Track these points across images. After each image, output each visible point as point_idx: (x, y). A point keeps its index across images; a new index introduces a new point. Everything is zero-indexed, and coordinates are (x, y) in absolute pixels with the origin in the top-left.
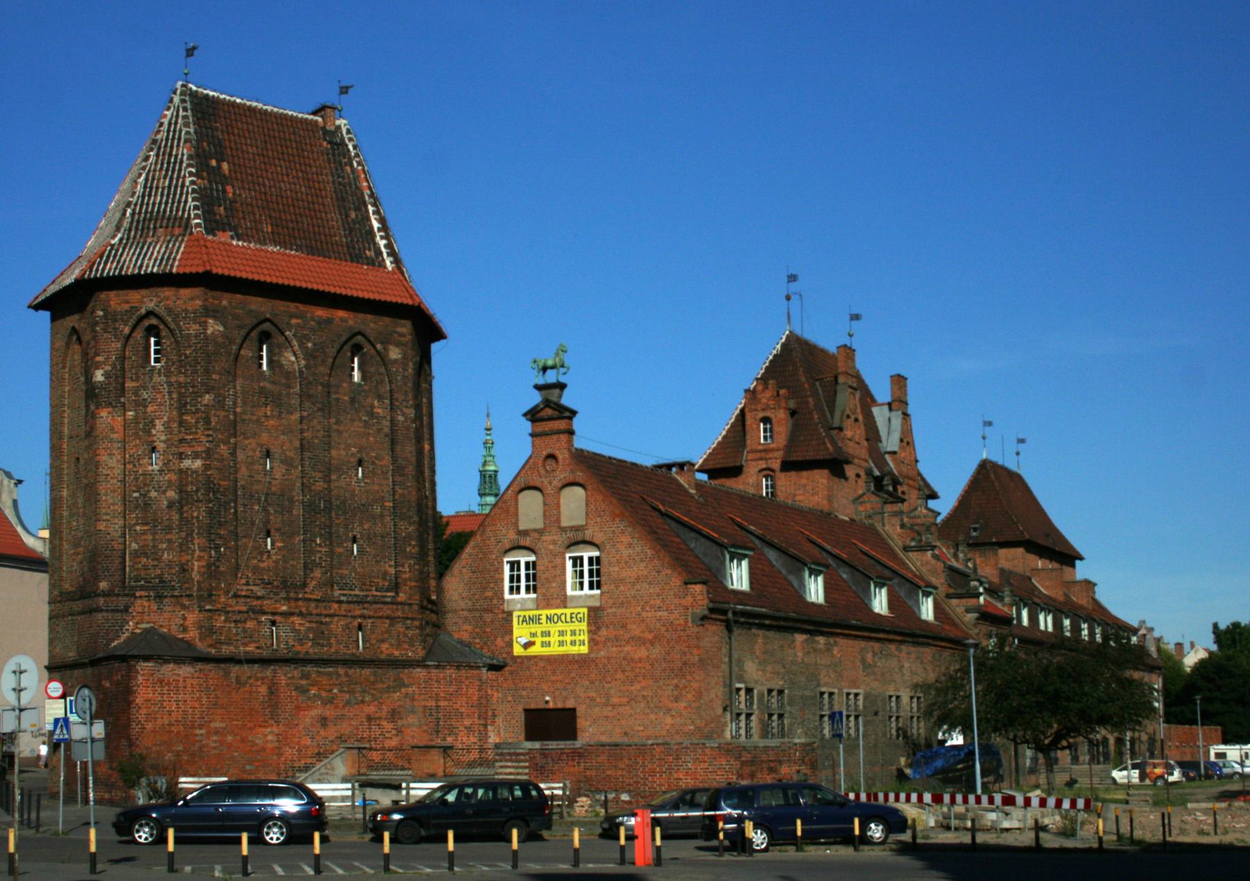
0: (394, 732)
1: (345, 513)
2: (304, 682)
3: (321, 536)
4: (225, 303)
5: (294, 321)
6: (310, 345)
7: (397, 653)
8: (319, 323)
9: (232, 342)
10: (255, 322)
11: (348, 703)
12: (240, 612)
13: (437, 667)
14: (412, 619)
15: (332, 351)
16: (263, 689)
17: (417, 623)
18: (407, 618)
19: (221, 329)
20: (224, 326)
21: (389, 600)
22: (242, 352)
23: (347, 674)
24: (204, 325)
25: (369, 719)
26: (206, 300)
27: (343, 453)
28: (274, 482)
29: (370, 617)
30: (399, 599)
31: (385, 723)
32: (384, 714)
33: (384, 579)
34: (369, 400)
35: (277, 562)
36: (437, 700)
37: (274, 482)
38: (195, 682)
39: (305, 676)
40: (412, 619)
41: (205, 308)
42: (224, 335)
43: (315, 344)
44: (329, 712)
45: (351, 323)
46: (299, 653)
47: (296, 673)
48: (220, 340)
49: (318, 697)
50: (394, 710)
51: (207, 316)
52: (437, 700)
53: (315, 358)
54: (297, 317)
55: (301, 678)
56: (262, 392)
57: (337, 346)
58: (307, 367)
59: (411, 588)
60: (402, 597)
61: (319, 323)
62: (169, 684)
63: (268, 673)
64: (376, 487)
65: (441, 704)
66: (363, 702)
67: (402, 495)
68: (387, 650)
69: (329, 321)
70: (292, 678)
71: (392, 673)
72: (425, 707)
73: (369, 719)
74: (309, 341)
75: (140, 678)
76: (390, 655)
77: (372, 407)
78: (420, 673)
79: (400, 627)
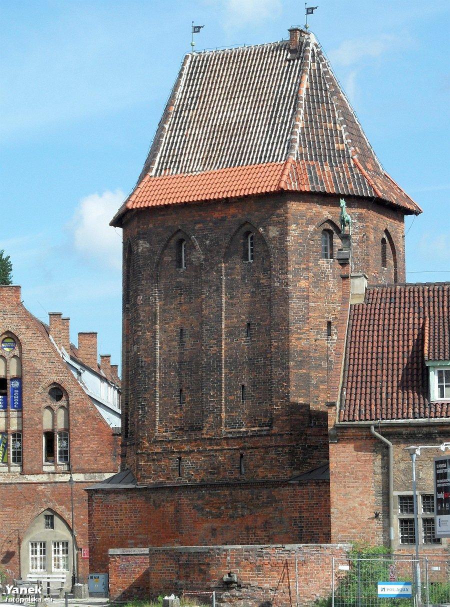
0: (266, 539)
1: (236, 368)
2: (200, 502)
3: (214, 388)
4: (151, 226)
5: (197, 226)
6: (208, 242)
7: (270, 476)
8: (215, 223)
9: (154, 253)
10: (171, 234)
11: (232, 517)
12: (156, 453)
13: (300, 484)
14: (283, 446)
15: (225, 243)
16: (171, 509)
17: (286, 450)
18: (279, 446)
19: (148, 246)
20: (150, 243)
21: (265, 433)
22: (165, 259)
23: (231, 494)
24: (137, 244)
25: (247, 528)
26: (139, 227)
27: (235, 320)
28: (186, 353)
29: (249, 448)
30: (273, 432)
31: (259, 532)
32: (259, 523)
33: (266, 416)
34: (256, 274)
35: (186, 413)
36: (301, 512)
37: (186, 353)
38: (127, 506)
39: (201, 498)
40: (283, 446)
41: (138, 233)
42: (150, 251)
43: (211, 241)
44: (217, 524)
45: (240, 216)
46: (196, 480)
47: (195, 496)
48: (147, 254)
49: (210, 513)
50: (266, 522)
51: (139, 239)
52: (301, 512)
53: (211, 251)
54: (199, 223)
55: (198, 499)
56: (179, 286)
57: (228, 238)
58: (205, 260)
59: (283, 421)
60: (275, 430)
61: (215, 223)
62: (111, 508)
63: (176, 496)
64: (261, 344)
65: (304, 514)
66: (243, 516)
67: (277, 347)
68: (262, 473)
69: (223, 219)
70: (192, 499)
71: (265, 492)
72: (291, 517)
73: (247, 528)
74: (207, 239)
75: (94, 505)
76: (264, 477)
77: (259, 279)
78: (286, 491)
79: (272, 454)
